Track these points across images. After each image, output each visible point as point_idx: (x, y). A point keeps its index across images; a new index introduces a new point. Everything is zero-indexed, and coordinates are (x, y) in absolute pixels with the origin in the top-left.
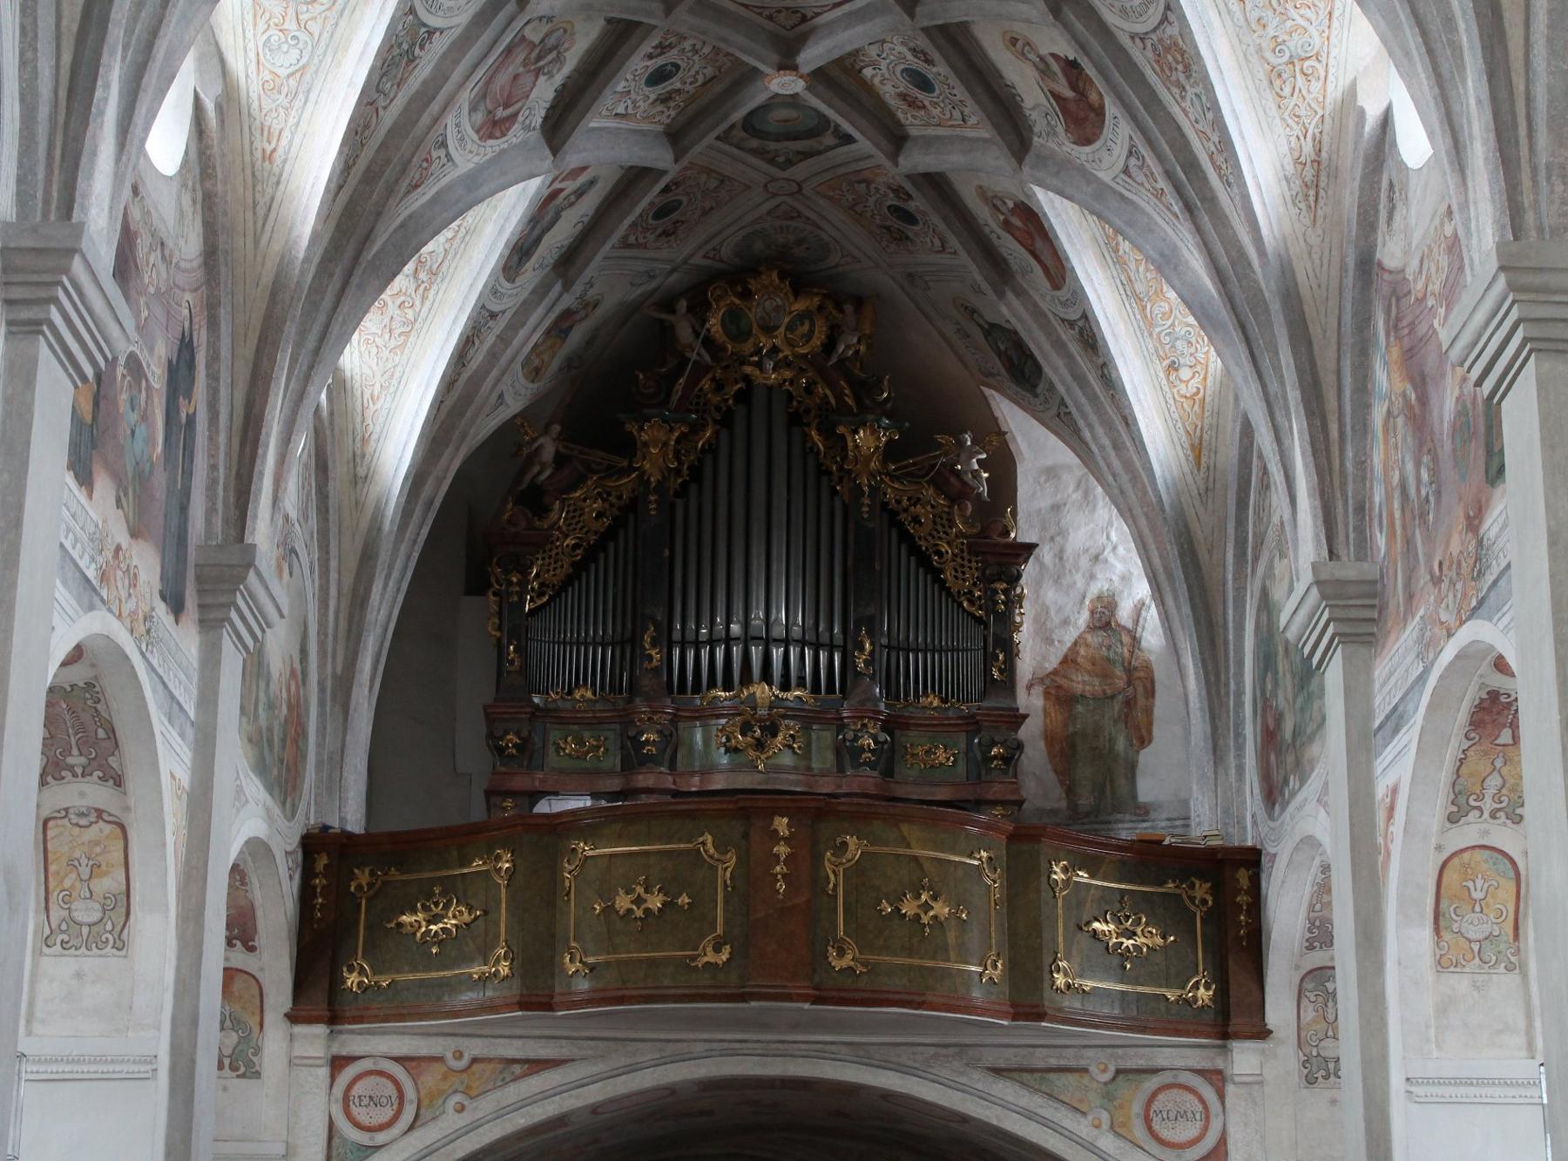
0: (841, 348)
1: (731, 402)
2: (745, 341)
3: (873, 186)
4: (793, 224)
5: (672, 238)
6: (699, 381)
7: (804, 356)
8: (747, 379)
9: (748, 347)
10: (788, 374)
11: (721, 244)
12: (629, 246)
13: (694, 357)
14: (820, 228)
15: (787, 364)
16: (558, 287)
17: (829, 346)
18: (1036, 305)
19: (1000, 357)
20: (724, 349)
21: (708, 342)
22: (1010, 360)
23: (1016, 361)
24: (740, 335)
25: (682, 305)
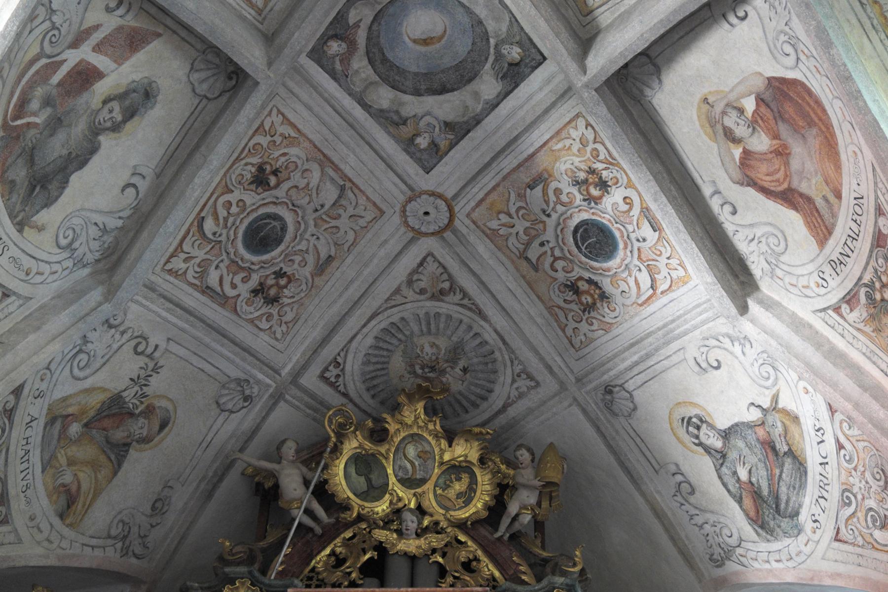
0: (513, 508)
1: (354, 575)
2: (378, 498)
3: (553, 185)
4: (443, 307)
5: (274, 311)
6: (311, 557)
7: (461, 525)
8: (380, 548)
9: (382, 507)
10: (435, 541)
11: (345, 349)
12: (207, 290)
13: (299, 516)
14: (481, 313)
15: (435, 528)
16: (96, 295)
17: (497, 509)
18: (793, 316)
19: (740, 501)
20: (346, 507)
21: (322, 493)
22: (756, 494)
23: (764, 485)
24: (375, 491)
25: (289, 450)
